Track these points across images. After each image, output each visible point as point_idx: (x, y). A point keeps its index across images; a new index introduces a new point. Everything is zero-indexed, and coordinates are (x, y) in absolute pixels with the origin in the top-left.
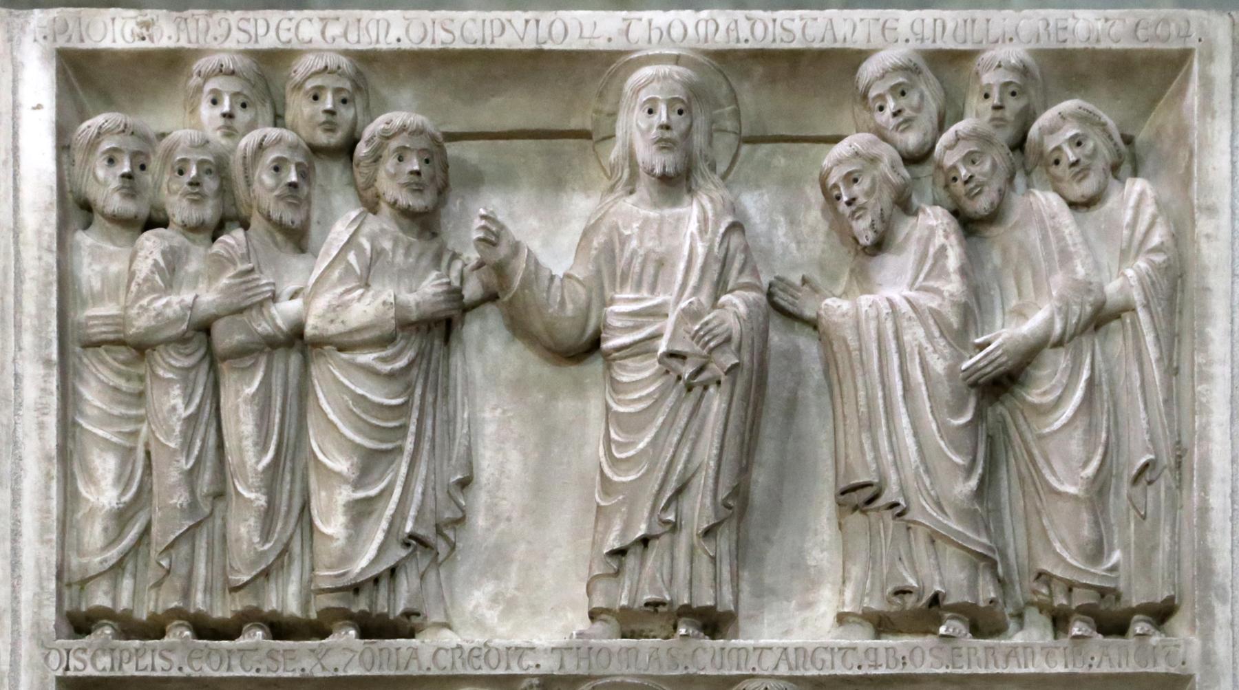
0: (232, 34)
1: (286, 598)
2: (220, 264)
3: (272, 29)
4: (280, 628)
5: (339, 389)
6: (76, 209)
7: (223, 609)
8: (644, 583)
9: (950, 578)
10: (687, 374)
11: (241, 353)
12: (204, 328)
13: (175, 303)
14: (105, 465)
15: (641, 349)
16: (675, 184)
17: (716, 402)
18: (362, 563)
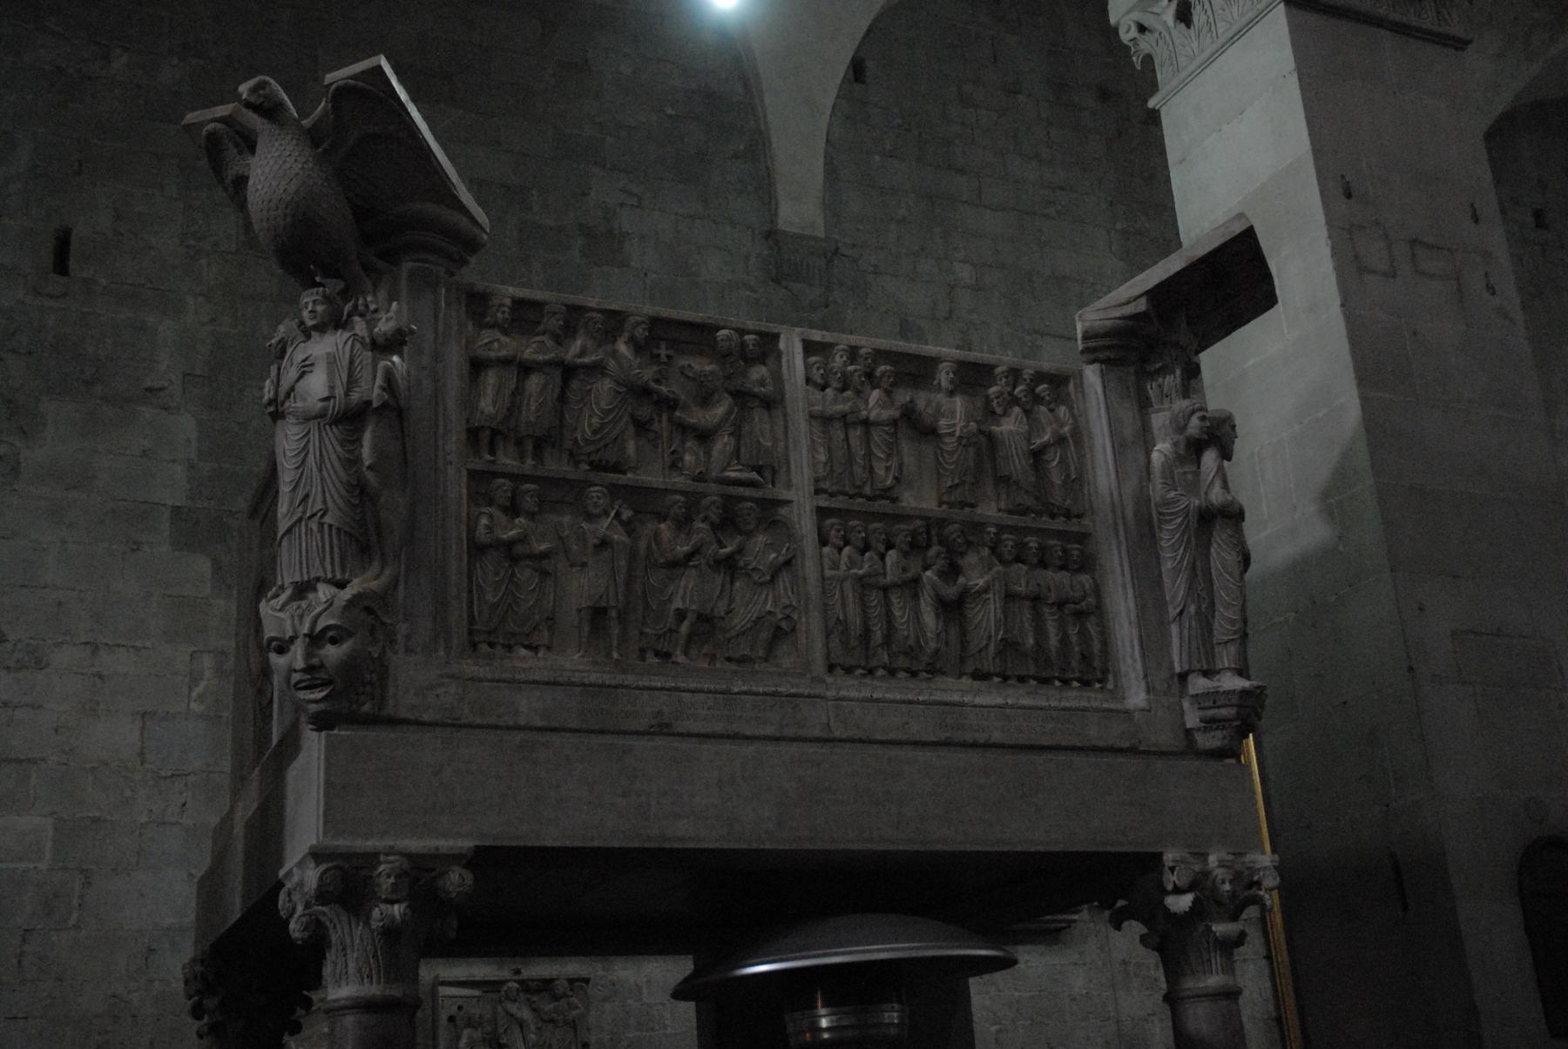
0: (845, 340)
1: (867, 490)
2: (849, 399)
3: (854, 339)
4: (869, 499)
5: (877, 436)
6: (808, 381)
7: (852, 491)
8: (956, 496)
9: (1029, 501)
10: (965, 441)
11: (854, 424)
12: (844, 416)
13: (839, 407)
14: (821, 449)
15: (952, 434)
16: (951, 393)
17: (971, 450)
18: (889, 482)
